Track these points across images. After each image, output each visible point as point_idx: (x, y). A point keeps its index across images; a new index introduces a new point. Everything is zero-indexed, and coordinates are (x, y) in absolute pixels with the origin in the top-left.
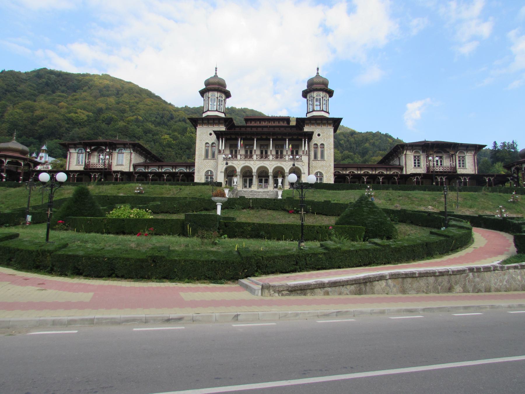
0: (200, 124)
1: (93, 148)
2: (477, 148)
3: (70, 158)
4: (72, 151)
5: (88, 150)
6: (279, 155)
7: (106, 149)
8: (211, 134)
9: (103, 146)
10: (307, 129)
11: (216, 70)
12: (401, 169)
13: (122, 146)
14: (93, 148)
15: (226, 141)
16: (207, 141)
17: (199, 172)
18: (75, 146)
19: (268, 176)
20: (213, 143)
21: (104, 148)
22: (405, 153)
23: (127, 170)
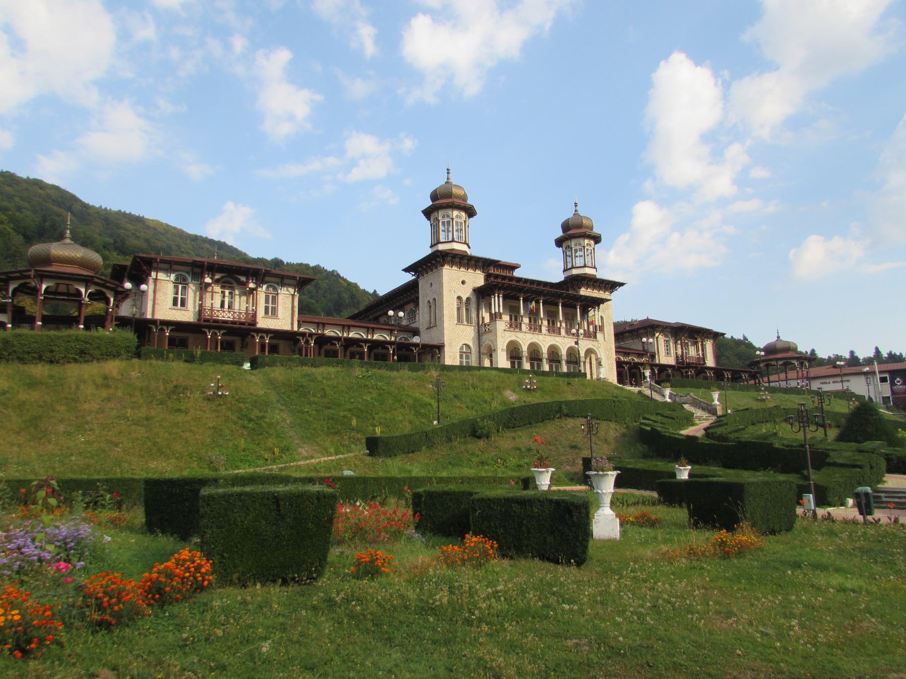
0: (448, 264)
1: (217, 277)
2: (716, 336)
3: (155, 292)
4: (161, 276)
5: (208, 280)
6: (535, 327)
7: (248, 282)
8: (463, 282)
9: (243, 275)
10: (584, 292)
11: (448, 173)
12: (653, 356)
13: (278, 280)
14: (217, 277)
15: (504, 298)
16: (460, 295)
17: (450, 345)
18: (169, 266)
19: (541, 360)
20: (468, 299)
21: (243, 279)
22: (657, 334)
23: (287, 327)
